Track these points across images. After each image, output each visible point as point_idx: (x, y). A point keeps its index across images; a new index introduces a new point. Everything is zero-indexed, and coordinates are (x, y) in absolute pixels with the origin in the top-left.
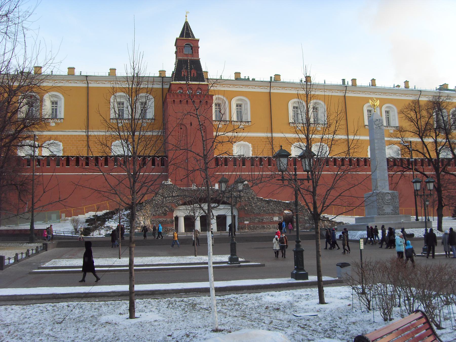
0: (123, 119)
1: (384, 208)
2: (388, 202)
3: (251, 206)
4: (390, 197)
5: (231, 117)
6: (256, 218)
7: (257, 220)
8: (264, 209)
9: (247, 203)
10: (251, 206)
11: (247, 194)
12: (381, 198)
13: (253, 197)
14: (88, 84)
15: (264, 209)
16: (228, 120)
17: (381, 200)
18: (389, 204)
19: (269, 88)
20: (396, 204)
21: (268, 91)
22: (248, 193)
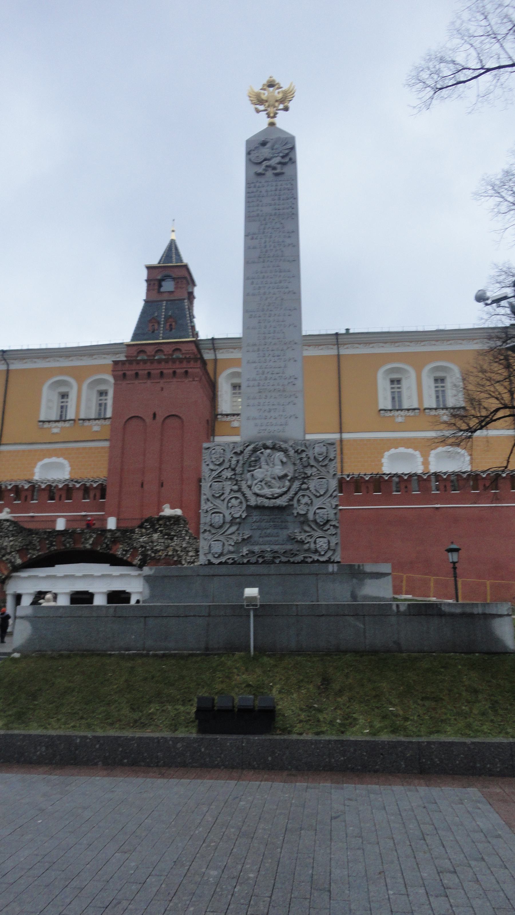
2: (267, 491)
4: (279, 470)
11: (172, 539)
12: (228, 474)
13: (185, 548)
14: (8, 364)
17: (228, 486)
19: (336, 346)
20: (318, 503)
21: (334, 352)
22: (175, 538)
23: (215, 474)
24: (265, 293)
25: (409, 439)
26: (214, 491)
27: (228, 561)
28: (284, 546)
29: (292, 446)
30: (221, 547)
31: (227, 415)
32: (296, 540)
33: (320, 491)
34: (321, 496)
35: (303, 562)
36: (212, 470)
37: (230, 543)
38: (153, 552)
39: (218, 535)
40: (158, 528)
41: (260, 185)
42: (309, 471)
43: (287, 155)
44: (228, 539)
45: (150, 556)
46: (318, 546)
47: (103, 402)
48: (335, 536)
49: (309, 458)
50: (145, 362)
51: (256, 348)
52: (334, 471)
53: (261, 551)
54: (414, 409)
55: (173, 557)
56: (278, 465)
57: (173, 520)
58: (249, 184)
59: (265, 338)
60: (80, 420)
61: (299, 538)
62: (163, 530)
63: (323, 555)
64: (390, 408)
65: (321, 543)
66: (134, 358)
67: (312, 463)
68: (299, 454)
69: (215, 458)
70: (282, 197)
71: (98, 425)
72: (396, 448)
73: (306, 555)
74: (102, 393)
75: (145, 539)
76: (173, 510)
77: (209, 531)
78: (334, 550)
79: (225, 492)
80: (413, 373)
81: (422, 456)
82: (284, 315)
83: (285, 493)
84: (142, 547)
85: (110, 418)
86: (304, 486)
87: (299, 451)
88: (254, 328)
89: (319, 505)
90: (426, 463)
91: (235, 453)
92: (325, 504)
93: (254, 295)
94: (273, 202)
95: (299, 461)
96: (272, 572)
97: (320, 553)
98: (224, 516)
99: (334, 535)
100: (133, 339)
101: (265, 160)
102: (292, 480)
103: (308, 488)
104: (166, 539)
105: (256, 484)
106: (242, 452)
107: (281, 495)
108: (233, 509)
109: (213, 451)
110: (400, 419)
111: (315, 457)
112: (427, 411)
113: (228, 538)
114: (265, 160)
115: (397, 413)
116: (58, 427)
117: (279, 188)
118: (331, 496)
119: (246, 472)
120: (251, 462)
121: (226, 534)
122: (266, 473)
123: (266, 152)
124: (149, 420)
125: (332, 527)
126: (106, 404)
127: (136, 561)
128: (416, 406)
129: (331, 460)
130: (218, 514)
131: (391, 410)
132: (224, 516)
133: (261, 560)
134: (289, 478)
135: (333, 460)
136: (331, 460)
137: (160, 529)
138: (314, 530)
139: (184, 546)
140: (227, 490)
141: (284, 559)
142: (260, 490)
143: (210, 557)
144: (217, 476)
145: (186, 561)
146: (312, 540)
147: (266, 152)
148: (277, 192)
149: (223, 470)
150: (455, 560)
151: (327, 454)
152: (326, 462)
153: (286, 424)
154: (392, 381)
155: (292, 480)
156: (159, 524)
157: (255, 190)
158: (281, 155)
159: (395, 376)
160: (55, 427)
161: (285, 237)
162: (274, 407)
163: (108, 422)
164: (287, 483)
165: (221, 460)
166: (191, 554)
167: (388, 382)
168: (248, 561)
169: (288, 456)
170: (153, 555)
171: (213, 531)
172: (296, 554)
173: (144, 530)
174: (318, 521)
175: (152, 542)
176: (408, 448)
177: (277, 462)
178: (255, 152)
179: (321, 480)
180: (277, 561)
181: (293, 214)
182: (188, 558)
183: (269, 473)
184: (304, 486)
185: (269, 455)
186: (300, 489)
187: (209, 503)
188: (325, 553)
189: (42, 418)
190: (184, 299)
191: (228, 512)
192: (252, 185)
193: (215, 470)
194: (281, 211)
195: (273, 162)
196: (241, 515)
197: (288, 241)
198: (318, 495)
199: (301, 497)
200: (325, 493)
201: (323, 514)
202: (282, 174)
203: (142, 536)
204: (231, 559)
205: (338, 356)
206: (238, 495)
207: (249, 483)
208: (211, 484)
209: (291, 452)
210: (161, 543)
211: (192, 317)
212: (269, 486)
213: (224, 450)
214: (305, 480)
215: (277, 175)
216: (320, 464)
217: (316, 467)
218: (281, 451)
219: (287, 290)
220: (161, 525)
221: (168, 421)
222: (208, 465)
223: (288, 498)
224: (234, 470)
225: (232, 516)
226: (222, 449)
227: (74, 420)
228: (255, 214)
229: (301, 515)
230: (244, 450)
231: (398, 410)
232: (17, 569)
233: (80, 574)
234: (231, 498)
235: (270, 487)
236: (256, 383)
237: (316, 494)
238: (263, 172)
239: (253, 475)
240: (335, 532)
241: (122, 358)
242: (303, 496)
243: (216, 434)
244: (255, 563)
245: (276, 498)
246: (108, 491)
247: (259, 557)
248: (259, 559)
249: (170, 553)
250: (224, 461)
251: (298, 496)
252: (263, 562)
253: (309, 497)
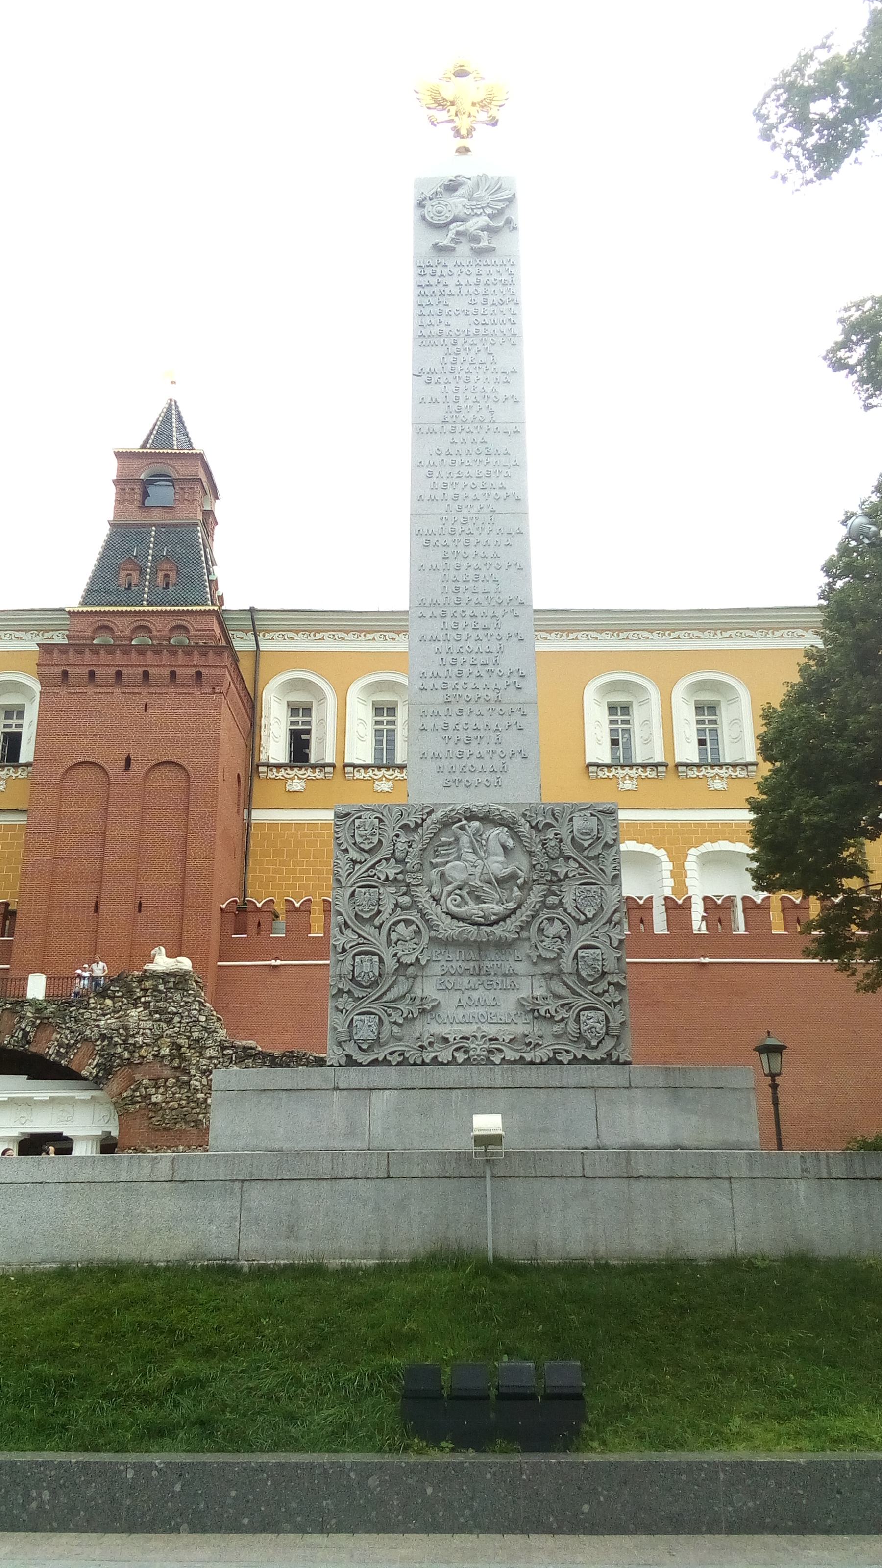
1: (428, 989)
2: (472, 908)
3: (188, 1083)
4: (497, 865)
9: (167, 1072)
11: (169, 1022)
13: (197, 1041)
16: (329, 759)
18: (503, 945)
20: (581, 936)
22: (177, 1019)
23: (360, 869)
24: (456, 498)
25: (645, 824)
26: (360, 908)
27: (388, 1058)
28: (511, 1028)
29: (524, 815)
30: (374, 1028)
31: (279, 767)
32: (536, 1014)
33: (586, 912)
34: (588, 920)
35: (553, 1061)
36: (355, 862)
37: (393, 1020)
38: (125, 1049)
39: (368, 1001)
40: (139, 998)
41: (446, 271)
42: (561, 869)
43: (501, 212)
44: (390, 1011)
45: (120, 1058)
46: (584, 1028)
48: (618, 1007)
49: (561, 841)
50: (110, 649)
51: (438, 612)
52: (615, 869)
53: (460, 1039)
54: (656, 766)
55: (171, 1061)
56: (497, 855)
57: (173, 979)
58: (422, 269)
59: (457, 591)
61: (543, 1013)
62: (150, 1002)
63: (597, 1047)
64: (608, 760)
65: (592, 1020)
66: (88, 642)
67: (569, 850)
68: (540, 831)
69: (361, 836)
70: (490, 299)
73: (557, 1047)
75: (109, 1021)
76: (173, 960)
77: (349, 992)
78: (618, 1037)
79: (382, 909)
80: (654, 695)
81: (671, 859)
82: (497, 545)
83: (514, 911)
84: (103, 1037)
85: (28, 765)
86: (552, 900)
87: (540, 827)
88: (435, 569)
89: (583, 941)
90: (679, 874)
91: (405, 827)
92: (598, 938)
93: (432, 499)
94: (472, 309)
95: (540, 846)
96: (499, 1083)
97: (588, 1042)
98: (381, 961)
99: (616, 1004)
100: (84, 603)
101: (455, 220)
102: (525, 887)
103: (561, 903)
104: (156, 1021)
105: (449, 894)
106: (418, 826)
107: (503, 919)
108: (399, 947)
109: (357, 822)
110: (628, 785)
111: (573, 837)
112: (680, 769)
113: (389, 1007)
114: (455, 220)
115: (621, 772)
117: (483, 279)
118: (610, 921)
119: (427, 866)
120: (438, 846)
121: (384, 999)
122: (471, 870)
123: (456, 204)
124: (115, 769)
125: (612, 988)
128: (659, 758)
129: (607, 846)
130: (367, 958)
131: (609, 766)
132: (381, 961)
133: (461, 1057)
134: (520, 881)
135: (612, 846)
136: (607, 846)
137: (143, 999)
138: (574, 992)
139: (195, 1035)
140: (388, 905)
141: (510, 1055)
142: (455, 906)
143: (351, 1049)
144: (367, 874)
145: (198, 1068)
146: (572, 1014)
147: (456, 204)
148: (481, 289)
149: (380, 861)
150: (776, 1070)
151: (599, 833)
152: (598, 850)
153: (504, 771)
154: (612, 709)
155: (525, 887)
156: (142, 990)
157: (433, 281)
158: (489, 211)
159: (620, 698)
161: (497, 382)
162: (479, 734)
163: (21, 774)
164: (516, 892)
165: (375, 840)
166: (209, 1053)
168: (436, 1057)
169: (515, 834)
170: (126, 1055)
171: (358, 993)
172: (538, 1044)
173: (108, 1002)
174: (584, 974)
175: (126, 1028)
176: (643, 842)
177: (494, 845)
178: (435, 202)
179: (588, 887)
180: (497, 1059)
181: (514, 335)
182: (204, 1062)
183: (478, 870)
184: (552, 900)
185: (477, 834)
186: (544, 905)
187: (348, 932)
188: (600, 1042)
190: (197, 525)
191: (392, 951)
192: (428, 271)
193: (361, 863)
194: (490, 329)
195: (474, 224)
196: (417, 959)
197: (503, 391)
198: (583, 918)
199: (545, 922)
200: (594, 915)
201: (594, 959)
202: (491, 250)
203: (104, 1015)
204: (396, 1054)
206: (413, 916)
207: (435, 890)
208: (354, 891)
209: (525, 828)
210: (144, 1029)
211: (211, 562)
212: (478, 897)
213: (381, 821)
214: (554, 888)
215: (479, 252)
216: (586, 852)
217: (575, 860)
218: (501, 825)
219: (502, 494)
220: (147, 990)
221: (156, 774)
222: (346, 851)
223: (518, 923)
224: (402, 861)
225: (398, 961)
226: (376, 818)
228: (435, 330)
229: (545, 959)
230: (423, 820)
231: (623, 766)
234: (396, 923)
235: (478, 900)
236: (439, 683)
237: (578, 917)
238: (452, 245)
239: (442, 874)
240: (620, 999)
241: (59, 639)
242: (551, 920)
243: (255, 803)
244: (449, 1063)
245: (491, 924)
246: (20, 918)
247: (457, 1050)
248: (456, 1054)
249: (165, 1051)
250: (380, 841)
251: (541, 920)
252: (467, 1062)
253: (563, 922)
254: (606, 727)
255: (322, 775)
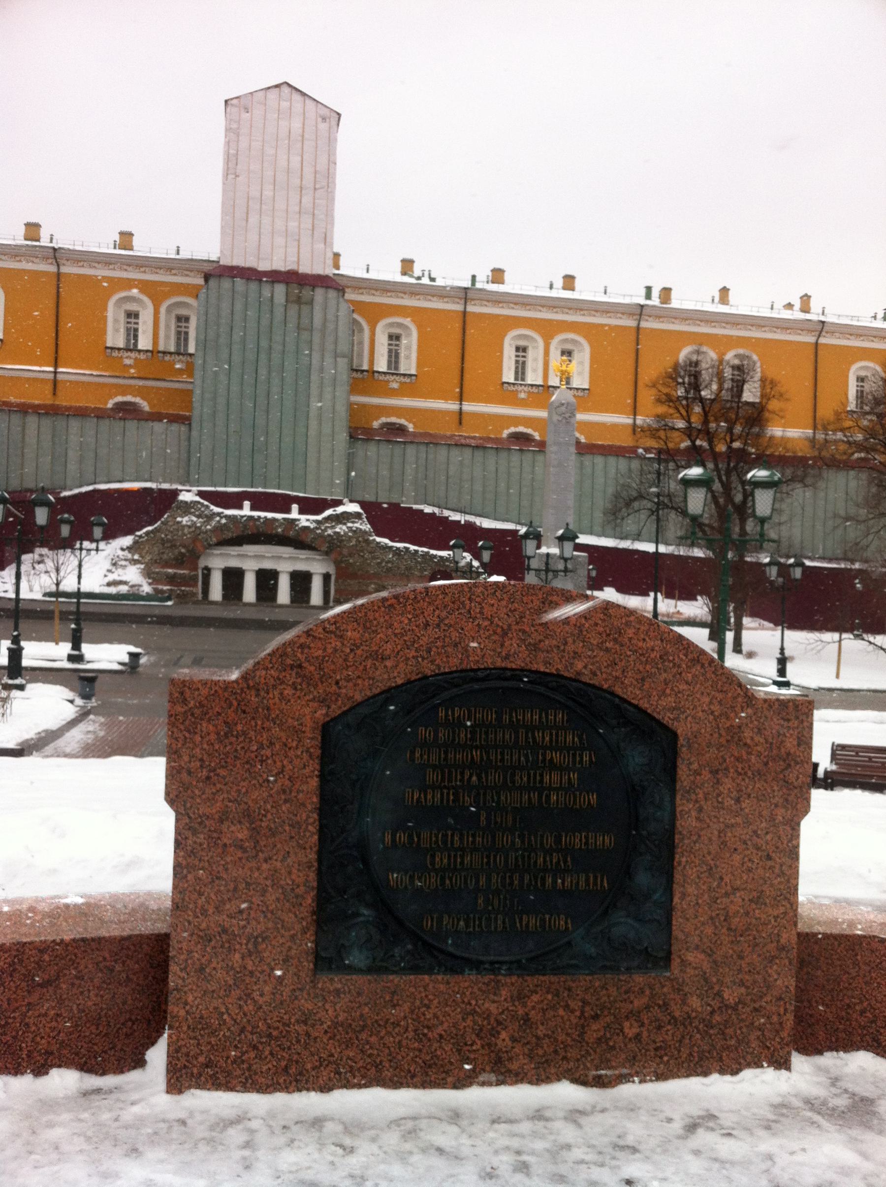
0: (135, 349)
5: (372, 362)
6: (371, 583)
7: (373, 586)
8: (390, 565)
10: (363, 556)
14: (58, 266)
15: (390, 565)
19: (463, 301)
20: (580, 579)
47: (183, 330)
60: (159, 352)
71: (182, 362)
72: (516, 426)
74: (182, 319)
110: (522, 395)
116: (131, 358)
126: (187, 333)
127: (324, 548)
159: (522, 343)
160: (127, 358)
167: (514, 349)
189: (109, 344)
205: (465, 313)
227: (152, 352)
232: (210, 546)
233: (270, 555)
254: (514, 358)
255: (361, 376)
